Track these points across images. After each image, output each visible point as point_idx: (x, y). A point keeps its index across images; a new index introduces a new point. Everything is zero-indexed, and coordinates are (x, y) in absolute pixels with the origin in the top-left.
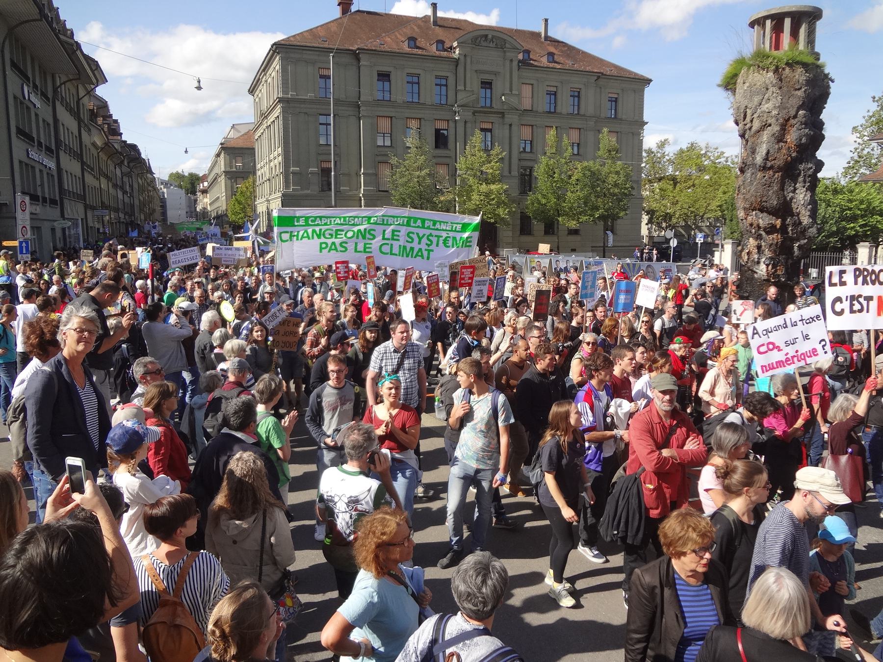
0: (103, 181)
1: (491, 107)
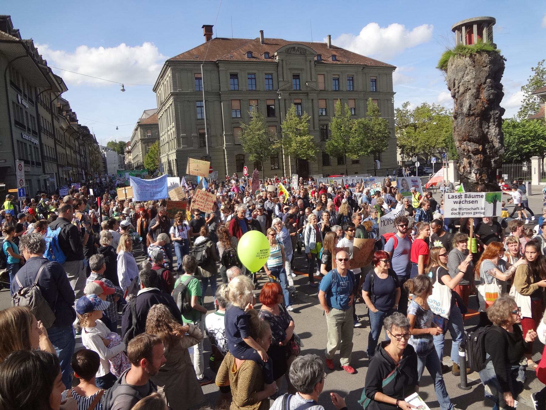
0: (68, 151)
1: (300, 90)
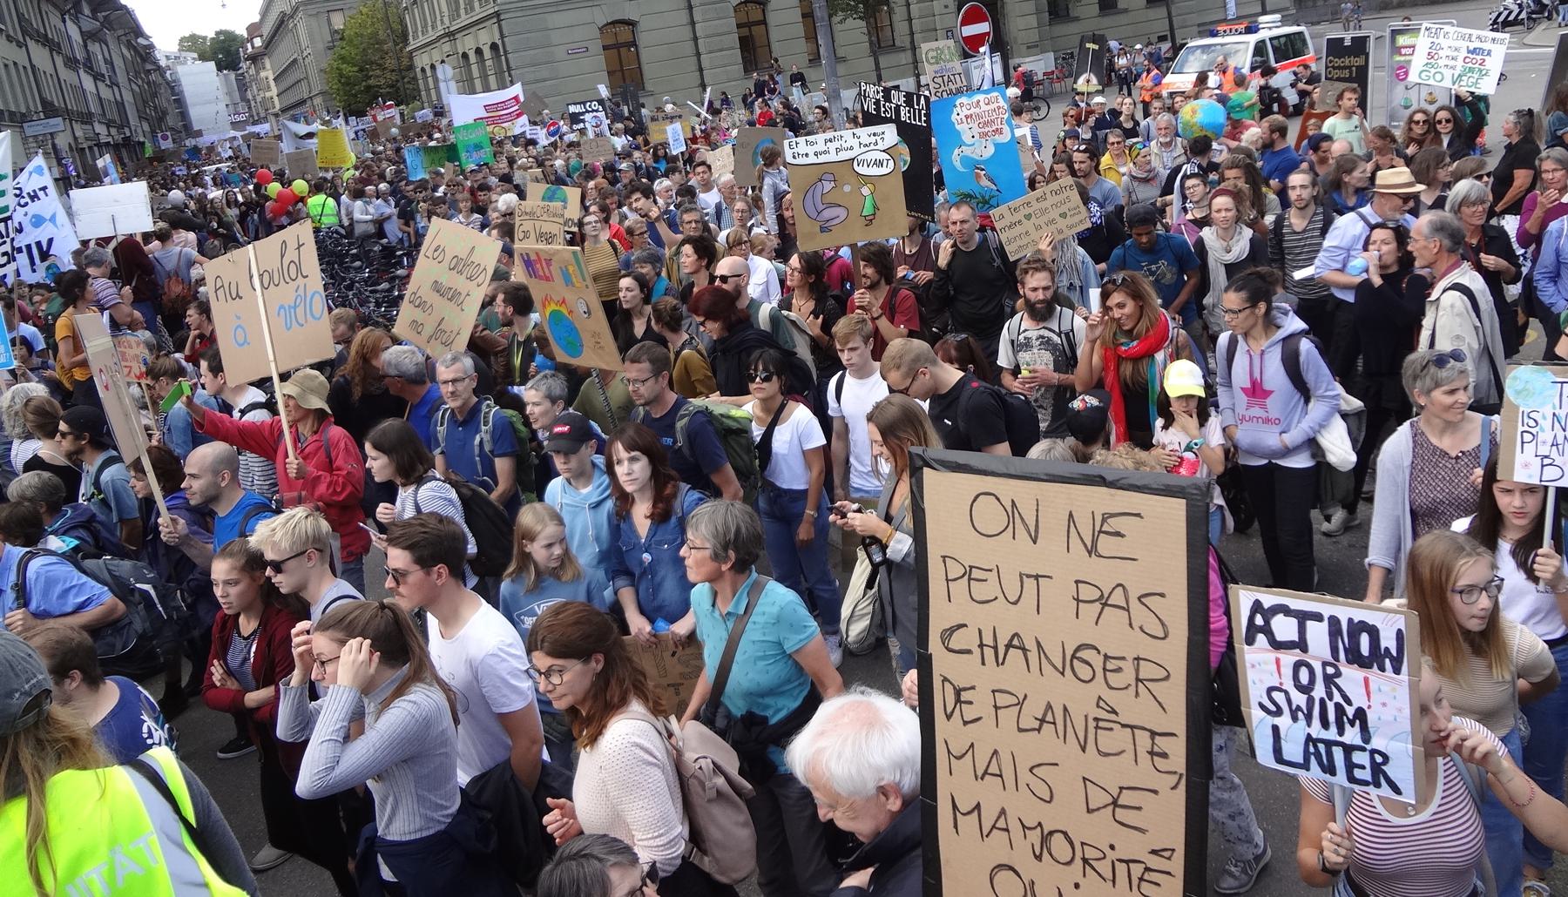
0: (40, 55)
